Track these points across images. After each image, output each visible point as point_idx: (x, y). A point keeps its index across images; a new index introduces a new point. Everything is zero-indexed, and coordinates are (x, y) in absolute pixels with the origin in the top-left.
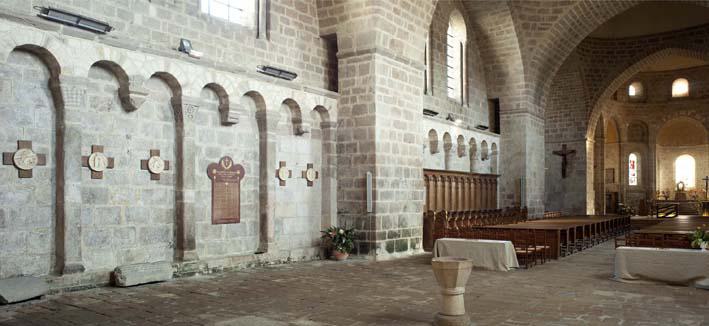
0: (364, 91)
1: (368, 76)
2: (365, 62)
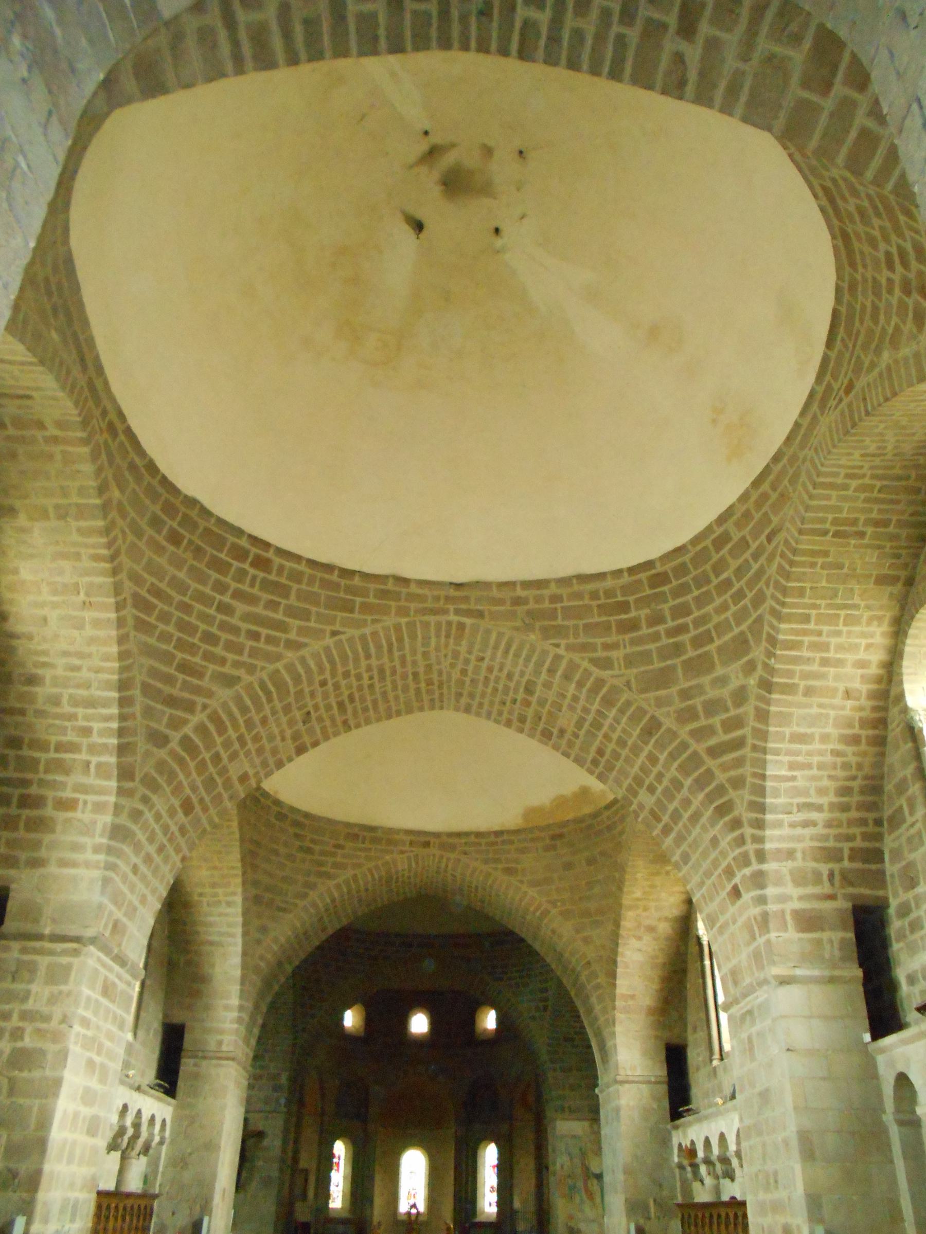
0: (47, 1018)
1: (63, 988)
2: (64, 960)
